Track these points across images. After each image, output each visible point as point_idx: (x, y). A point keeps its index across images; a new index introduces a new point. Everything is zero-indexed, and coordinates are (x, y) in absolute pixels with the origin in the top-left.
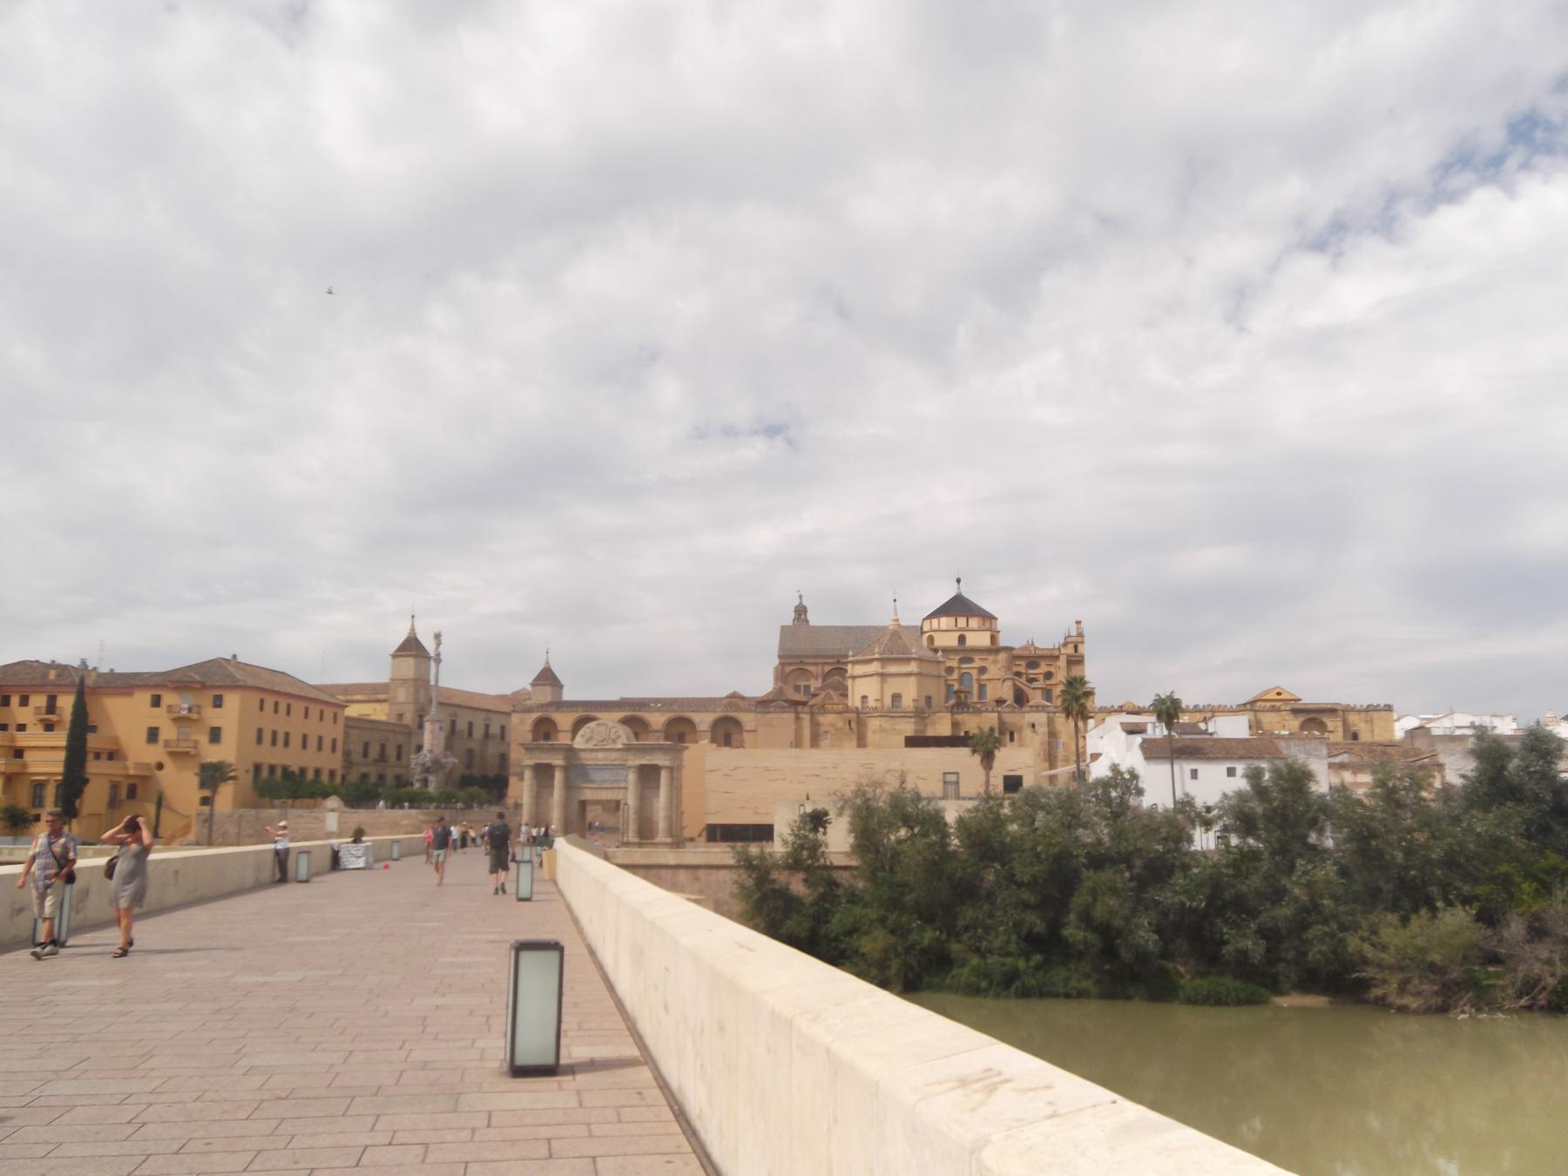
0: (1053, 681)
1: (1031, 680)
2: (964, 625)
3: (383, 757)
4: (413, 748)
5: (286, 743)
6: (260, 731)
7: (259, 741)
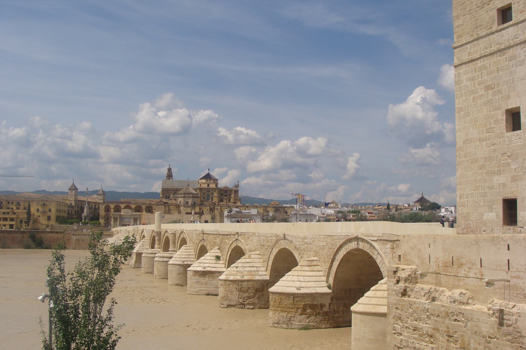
4: (74, 211)
5: (60, 212)
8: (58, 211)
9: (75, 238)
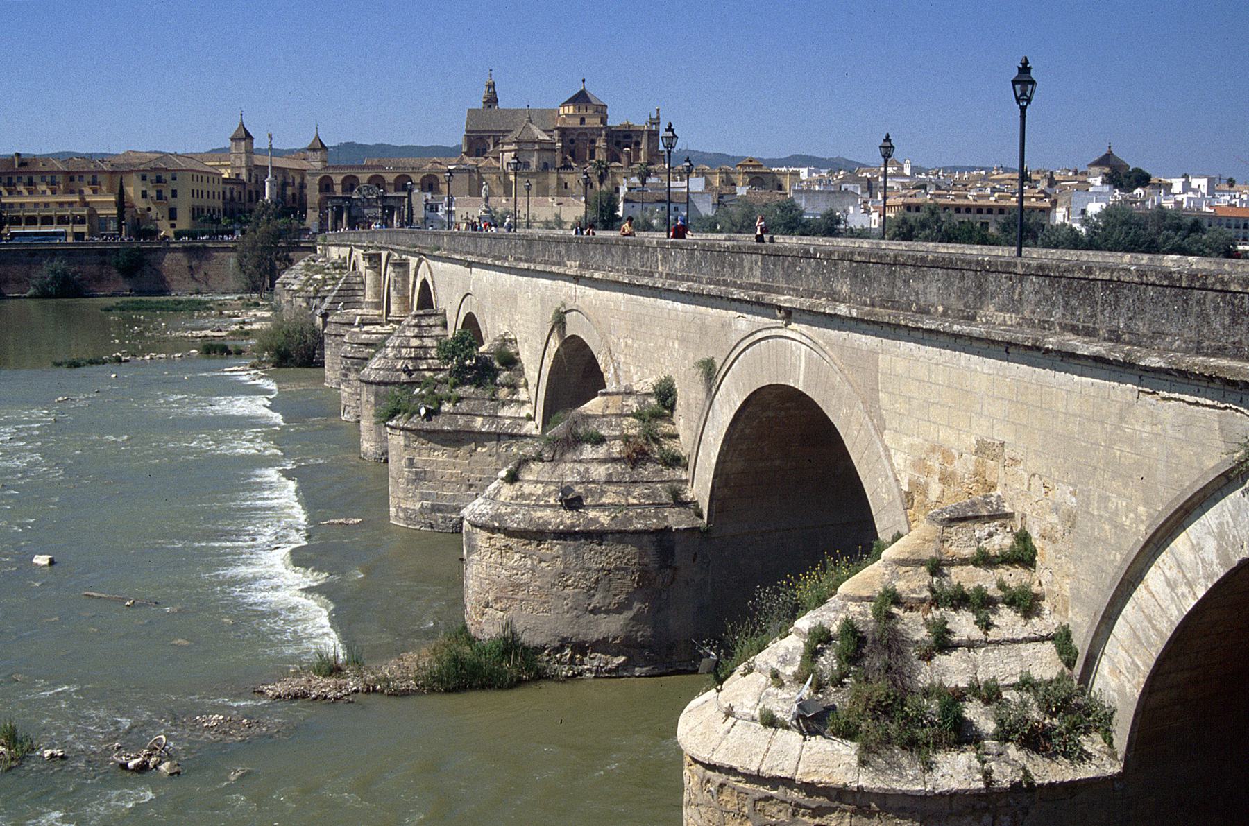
3: (232, 198)
4: (247, 193)
5: (202, 197)
6: (193, 190)
7: (193, 196)
8: (196, 195)
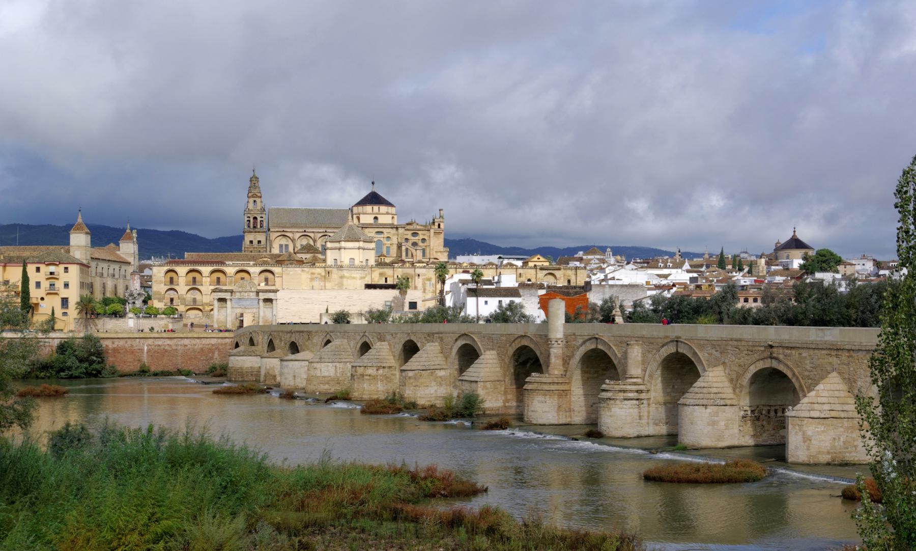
0: (425, 244)
1: (415, 244)
2: (377, 211)
9: (146, 348)
